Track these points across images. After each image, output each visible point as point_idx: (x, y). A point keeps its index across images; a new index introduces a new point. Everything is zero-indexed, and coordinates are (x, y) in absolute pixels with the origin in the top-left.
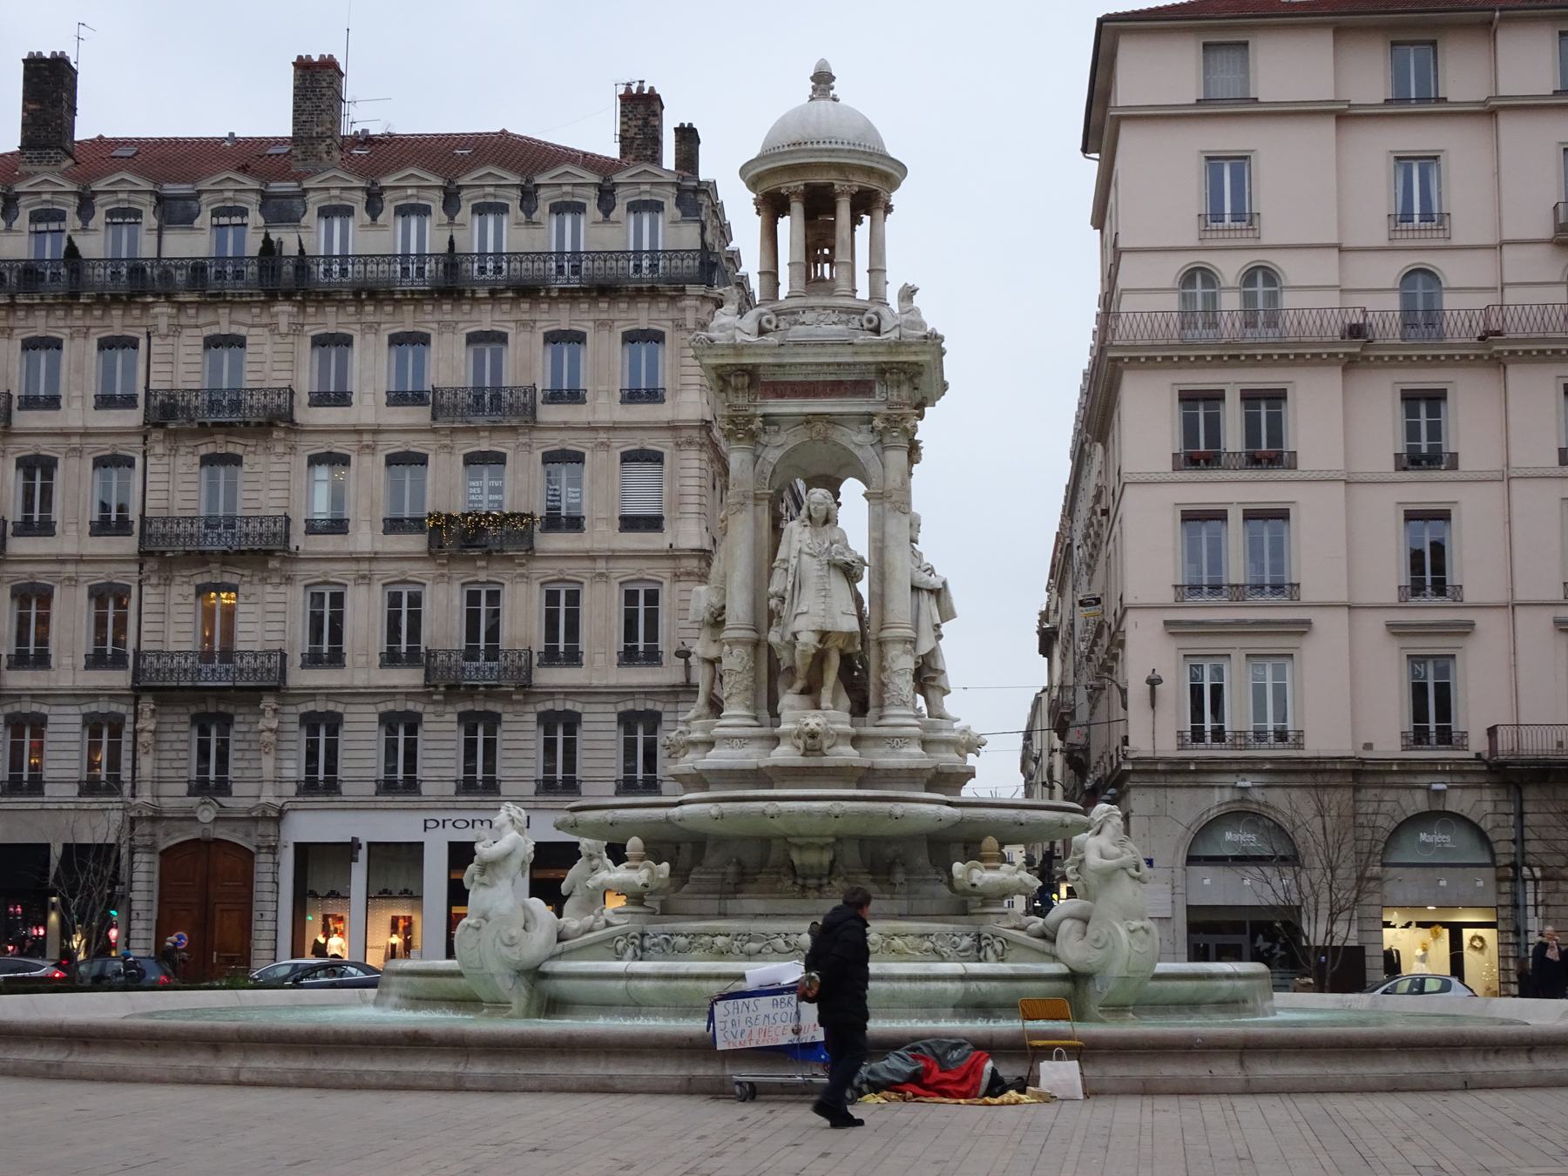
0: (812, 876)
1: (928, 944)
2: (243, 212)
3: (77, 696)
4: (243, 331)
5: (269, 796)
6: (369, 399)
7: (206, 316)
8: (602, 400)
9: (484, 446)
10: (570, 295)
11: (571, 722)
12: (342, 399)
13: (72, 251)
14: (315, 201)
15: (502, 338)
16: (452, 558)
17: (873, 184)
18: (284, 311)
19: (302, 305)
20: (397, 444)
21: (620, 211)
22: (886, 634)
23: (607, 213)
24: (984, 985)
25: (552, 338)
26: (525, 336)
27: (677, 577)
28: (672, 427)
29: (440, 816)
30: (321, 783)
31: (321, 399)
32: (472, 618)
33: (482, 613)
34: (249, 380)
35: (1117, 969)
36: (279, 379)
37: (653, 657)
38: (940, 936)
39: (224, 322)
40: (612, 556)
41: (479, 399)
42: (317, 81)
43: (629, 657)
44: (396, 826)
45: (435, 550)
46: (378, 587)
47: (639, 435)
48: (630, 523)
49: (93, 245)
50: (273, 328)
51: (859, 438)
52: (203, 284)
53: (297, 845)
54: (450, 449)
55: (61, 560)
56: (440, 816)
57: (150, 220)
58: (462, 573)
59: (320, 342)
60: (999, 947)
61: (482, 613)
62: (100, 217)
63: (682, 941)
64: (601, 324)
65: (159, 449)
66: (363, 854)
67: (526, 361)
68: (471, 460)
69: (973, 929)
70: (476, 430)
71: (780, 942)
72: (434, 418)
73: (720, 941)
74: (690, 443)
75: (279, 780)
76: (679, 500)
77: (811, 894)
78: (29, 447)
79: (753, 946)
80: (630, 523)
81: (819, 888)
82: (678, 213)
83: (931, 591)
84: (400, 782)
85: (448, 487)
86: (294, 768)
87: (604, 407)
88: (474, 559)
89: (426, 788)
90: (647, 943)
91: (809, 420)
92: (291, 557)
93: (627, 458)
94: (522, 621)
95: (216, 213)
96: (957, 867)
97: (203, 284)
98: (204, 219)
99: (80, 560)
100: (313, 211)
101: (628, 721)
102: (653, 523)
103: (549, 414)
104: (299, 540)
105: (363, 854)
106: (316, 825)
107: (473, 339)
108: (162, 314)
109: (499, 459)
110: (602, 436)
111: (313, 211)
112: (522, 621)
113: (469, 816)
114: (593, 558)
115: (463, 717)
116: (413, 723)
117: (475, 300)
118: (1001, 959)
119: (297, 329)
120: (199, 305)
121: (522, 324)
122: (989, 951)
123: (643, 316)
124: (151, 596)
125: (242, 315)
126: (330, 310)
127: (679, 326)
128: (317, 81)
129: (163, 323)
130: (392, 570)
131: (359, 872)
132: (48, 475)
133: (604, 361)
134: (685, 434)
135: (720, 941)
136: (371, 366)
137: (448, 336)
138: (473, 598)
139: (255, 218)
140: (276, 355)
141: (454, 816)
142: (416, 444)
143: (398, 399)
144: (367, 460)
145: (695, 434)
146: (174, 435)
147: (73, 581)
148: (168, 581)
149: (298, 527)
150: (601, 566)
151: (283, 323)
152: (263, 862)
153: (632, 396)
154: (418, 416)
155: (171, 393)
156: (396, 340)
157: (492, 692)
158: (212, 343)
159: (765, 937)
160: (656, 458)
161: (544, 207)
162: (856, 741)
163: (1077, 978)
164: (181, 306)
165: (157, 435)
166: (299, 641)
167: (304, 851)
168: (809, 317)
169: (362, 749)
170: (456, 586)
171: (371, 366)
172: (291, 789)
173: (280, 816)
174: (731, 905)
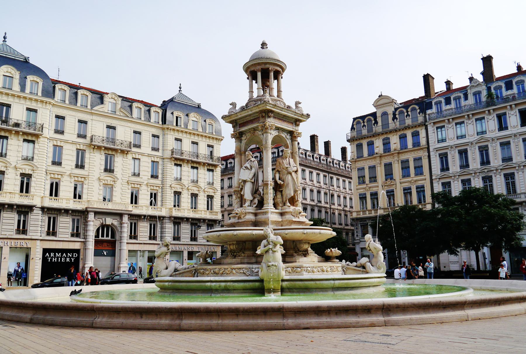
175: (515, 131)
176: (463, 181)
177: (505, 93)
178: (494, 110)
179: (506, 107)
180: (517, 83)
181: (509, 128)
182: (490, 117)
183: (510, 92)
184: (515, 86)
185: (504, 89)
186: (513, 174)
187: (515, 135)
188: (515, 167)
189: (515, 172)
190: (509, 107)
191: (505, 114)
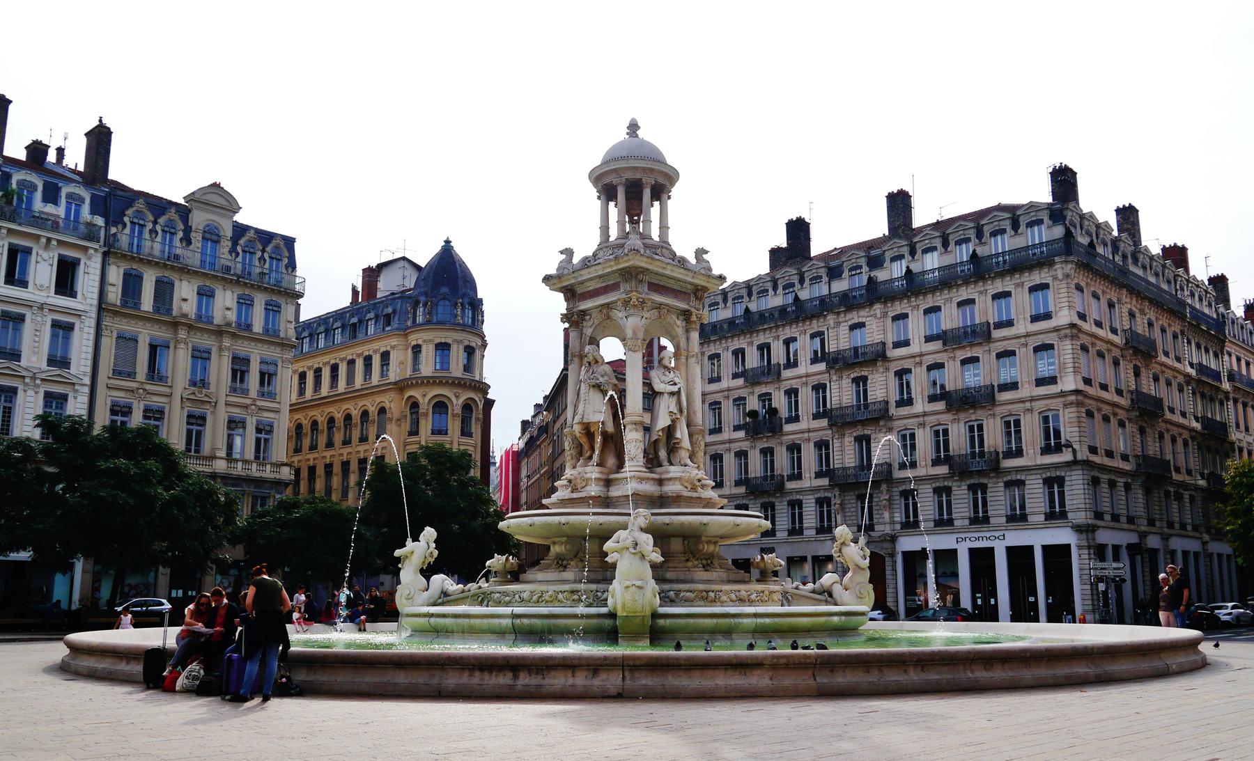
1: (576, 597)
2: (861, 267)
3: (814, 490)
4: (863, 320)
5: (887, 529)
6: (917, 341)
7: (849, 316)
8: (1021, 322)
9: (969, 355)
10: (1002, 275)
11: (1021, 484)
12: (906, 343)
13: (796, 298)
14: (888, 255)
15: (972, 301)
16: (958, 410)
18: (878, 308)
19: (885, 303)
20: (929, 360)
21: (1022, 228)
23: (1016, 232)
24: (526, 621)
25: (996, 297)
26: (982, 298)
27: (1065, 406)
28: (1056, 330)
29: (963, 536)
30: (911, 525)
31: (897, 345)
32: (972, 439)
33: (976, 432)
34: (868, 341)
36: (878, 338)
37: (1058, 449)
39: (854, 317)
40: (1032, 399)
41: (966, 333)
42: (899, 204)
43: (1046, 450)
44: (945, 541)
45: (949, 409)
46: (928, 429)
47: (1040, 336)
48: (1040, 382)
49: (804, 295)
50: (875, 316)
51: (620, 315)
52: (847, 302)
53: (904, 553)
54: (954, 358)
55: (802, 432)
56: (963, 536)
57: (825, 279)
58: (962, 416)
59: (896, 318)
61: (976, 432)
62: (807, 282)
64: (1017, 285)
65: (834, 378)
66: (931, 556)
67: (985, 311)
68: (964, 362)
70: (964, 347)
72: (944, 344)
74: (1066, 336)
75: (893, 523)
76: (1062, 367)
78: (787, 385)
79: (507, 599)
80: (1040, 382)
82: (1050, 222)
83: (672, 394)
84: (944, 523)
85: (955, 377)
86: (899, 517)
87: (1023, 326)
88: (967, 410)
89: (956, 523)
92: (891, 419)
93: (1037, 349)
94: (994, 437)
95: (850, 270)
97: (847, 302)
98: (846, 274)
99: (809, 431)
100: (888, 260)
101: (1048, 482)
102: (1052, 380)
103: (997, 334)
104: (893, 411)
105: (931, 556)
106: (909, 543)
107: (960, 304)
108: (831, 319)
109: (975, 360)
110: (1023, 340)
111: (888, 260)
112: (994, 437)
113: (977, 535)
114: (1023, 402)
115: (970, 487)
116: (948, 490)
117: (958, 286)
119: (885, 315)
120: (845, 312)
121: (981, 293)
123: (1037, 277)
124: (837, 444)
125: (863, 313)
126: (897, 303)
127: (1055, 278)
128: (899, 204)
129: (832, 322)
130: (931, 420)
131: (930, 565)
132: (796, 396)
133: (1021, 304)
134: (1063, 332)
136: (917, 327)
137: (948, 305)
138: (971, 429)
139: (865, 269)
140: (876, 327)
141: (969, 535)
142: (939, 358)
143: (929, 339)
144: (918, 369)
145: (1068, 331)
146: (840, 370)
147: (808, 440)
148: (843, 436)
149: (893, 404)
150: (1028, 405)
151: (878, 312)
152: (888, 561)
153: (1035, 319)
154: (937, 345)
155: (838, 352)
156: (927, 312)
157: (981, 473)
158: (853, 327)
160: (1051, 347)
161: (987, 234)
164: (838, 313)
165: (832, 372)
166: (898, 455)
167: (906, 555)
169: (927, 507)
170: (962, 424)
171: (917, 327)
172: (898, 527)
173: (893, 539)
175: (40, 297)
176: (48, 395)
177: (38, 205)
178: (10, 231)
179: (38, 237)
180: (69, 196)
181: (31, 285)
182: (45, 255)
183: (50, 208)
184: (63, 201)
185: (38, 195)
186: (14, 391)
187: (41, 307)
188: (24, 377)
189: (21, 388)
190: (44, 240)
191: (28, 251)
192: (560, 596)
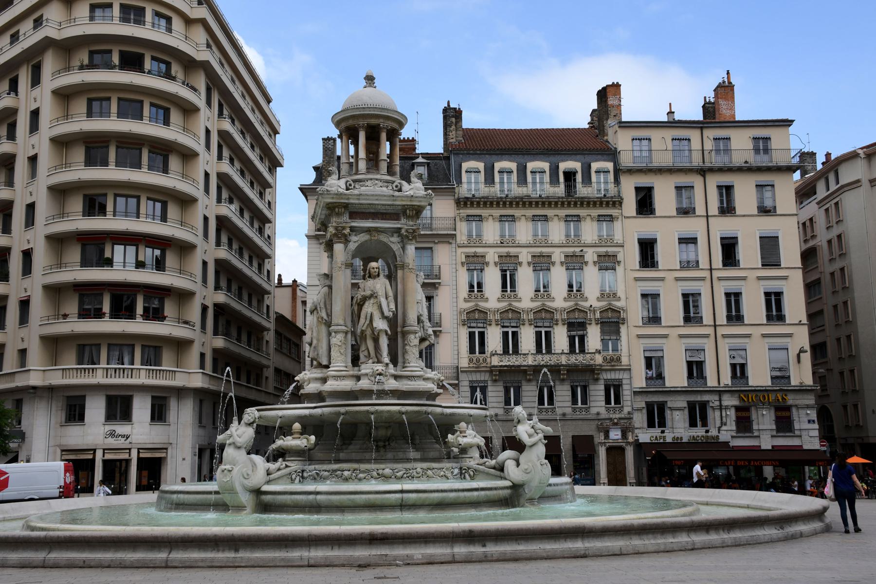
0: (380, 440)
1: (442, 473)
17: (396, 126)
22: (406, 329)
35: (535, 483)
38: (447, 469)
51: (392, 239)
60: (472, 473)
63: (326, 473)
69: (458, 465)
71: (375, 474)
73: (346, 473)
77: (382, 450)
79: (361, 475)
81: (384, 446)
90: (305, 475)
91: (369, 230)
96: (450, 436)
118: (472, 478)
122: (467, 475)
135: (346, 473)
159: (367, 471)
162: (396, 377)
163: (516, 487)
168: (369, 183)
174: (342, 455)
192: (430, 472)
